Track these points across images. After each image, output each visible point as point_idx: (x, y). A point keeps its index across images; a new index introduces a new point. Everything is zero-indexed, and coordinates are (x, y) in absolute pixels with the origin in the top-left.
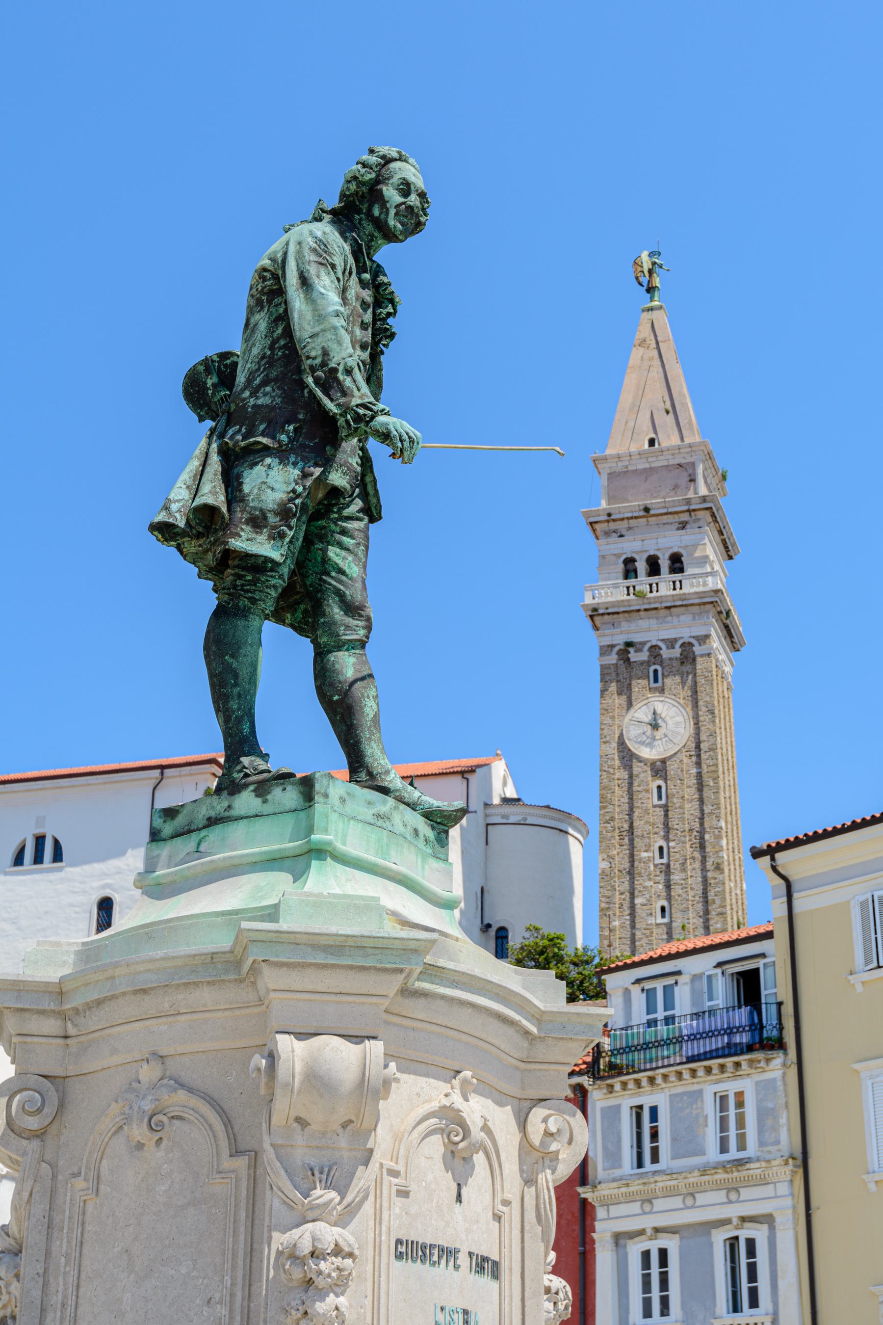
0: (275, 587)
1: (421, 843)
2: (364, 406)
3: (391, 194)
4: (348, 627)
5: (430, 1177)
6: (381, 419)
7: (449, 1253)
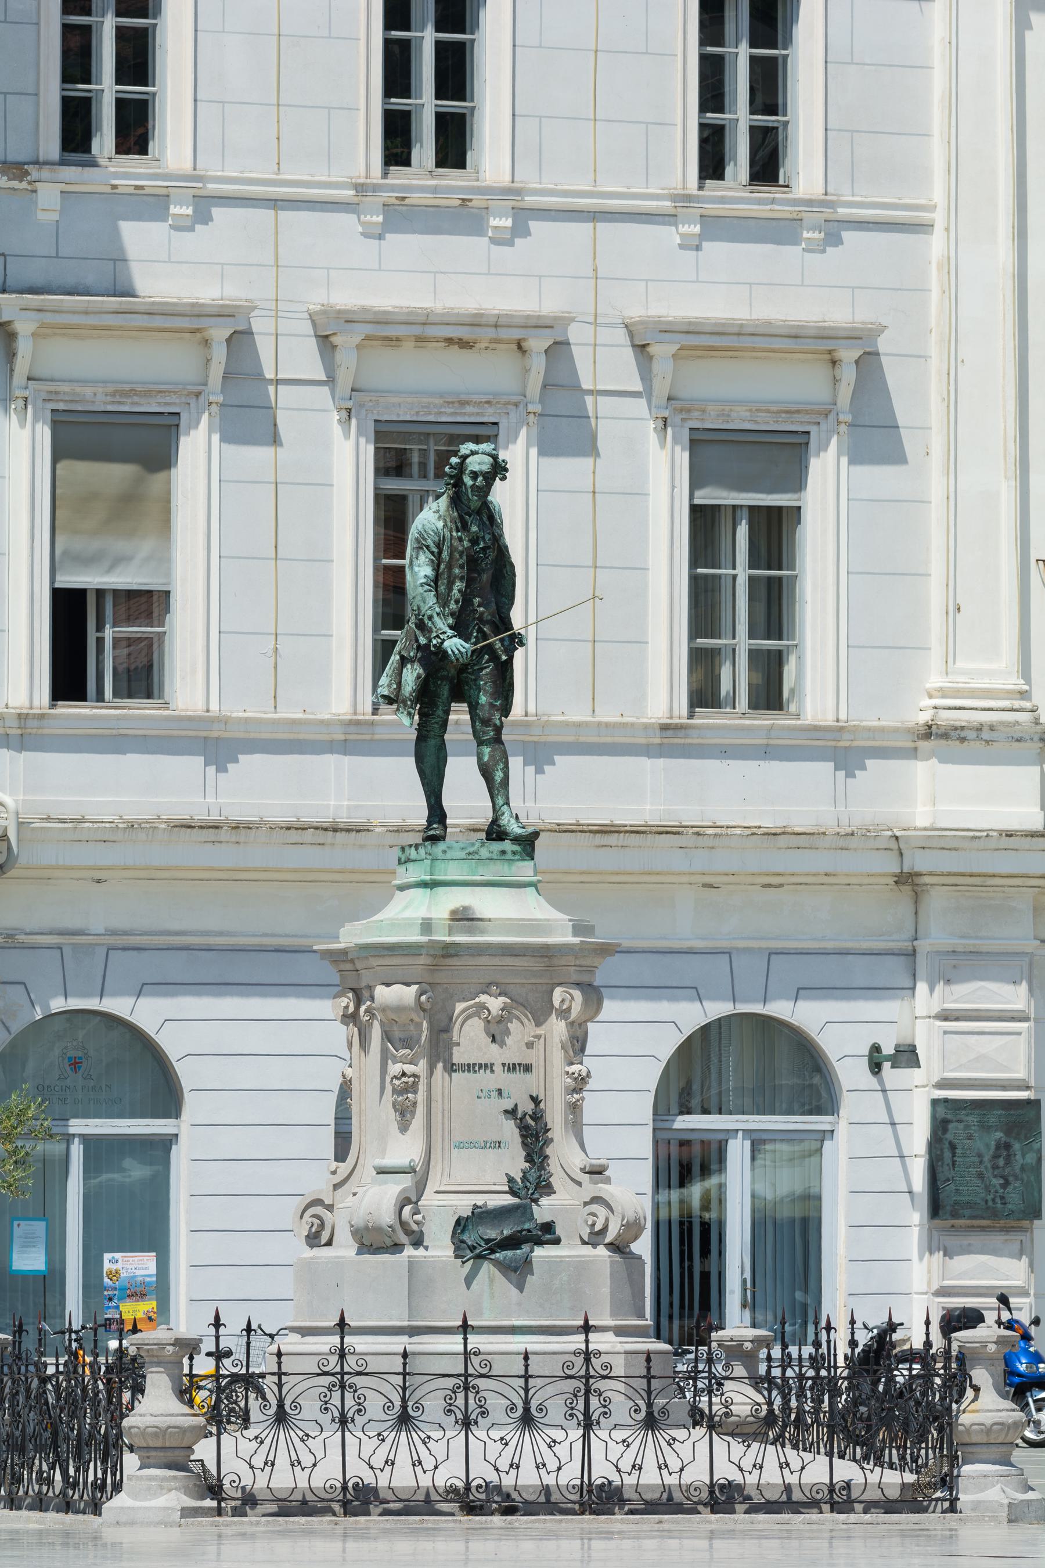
0: (436, 723)
1: (509, 856)
2: (438, 636)
3: (468, 481)
4: (484, 733)
5: (472, 1034)
6: (446, 644)
7: (489, 1067)
